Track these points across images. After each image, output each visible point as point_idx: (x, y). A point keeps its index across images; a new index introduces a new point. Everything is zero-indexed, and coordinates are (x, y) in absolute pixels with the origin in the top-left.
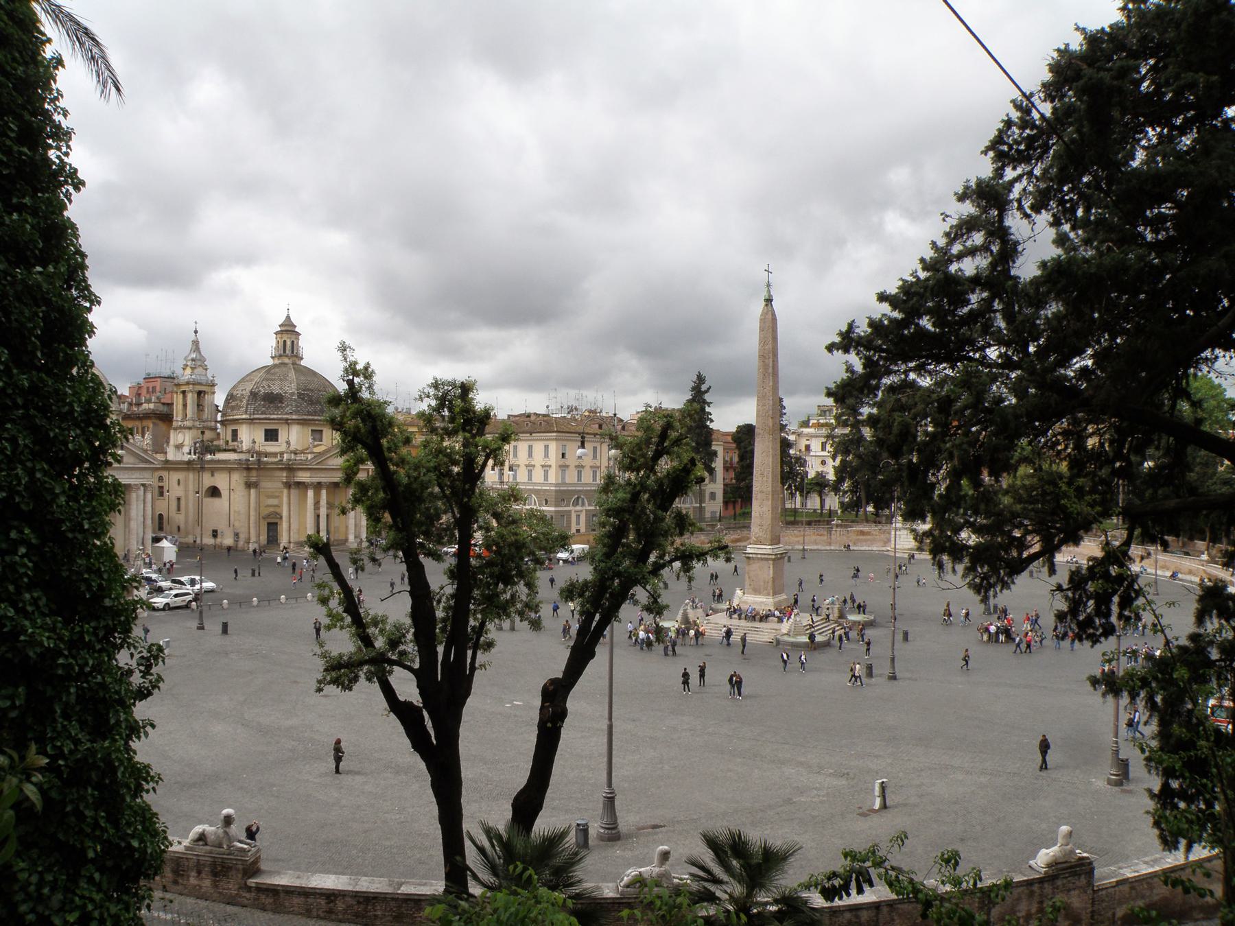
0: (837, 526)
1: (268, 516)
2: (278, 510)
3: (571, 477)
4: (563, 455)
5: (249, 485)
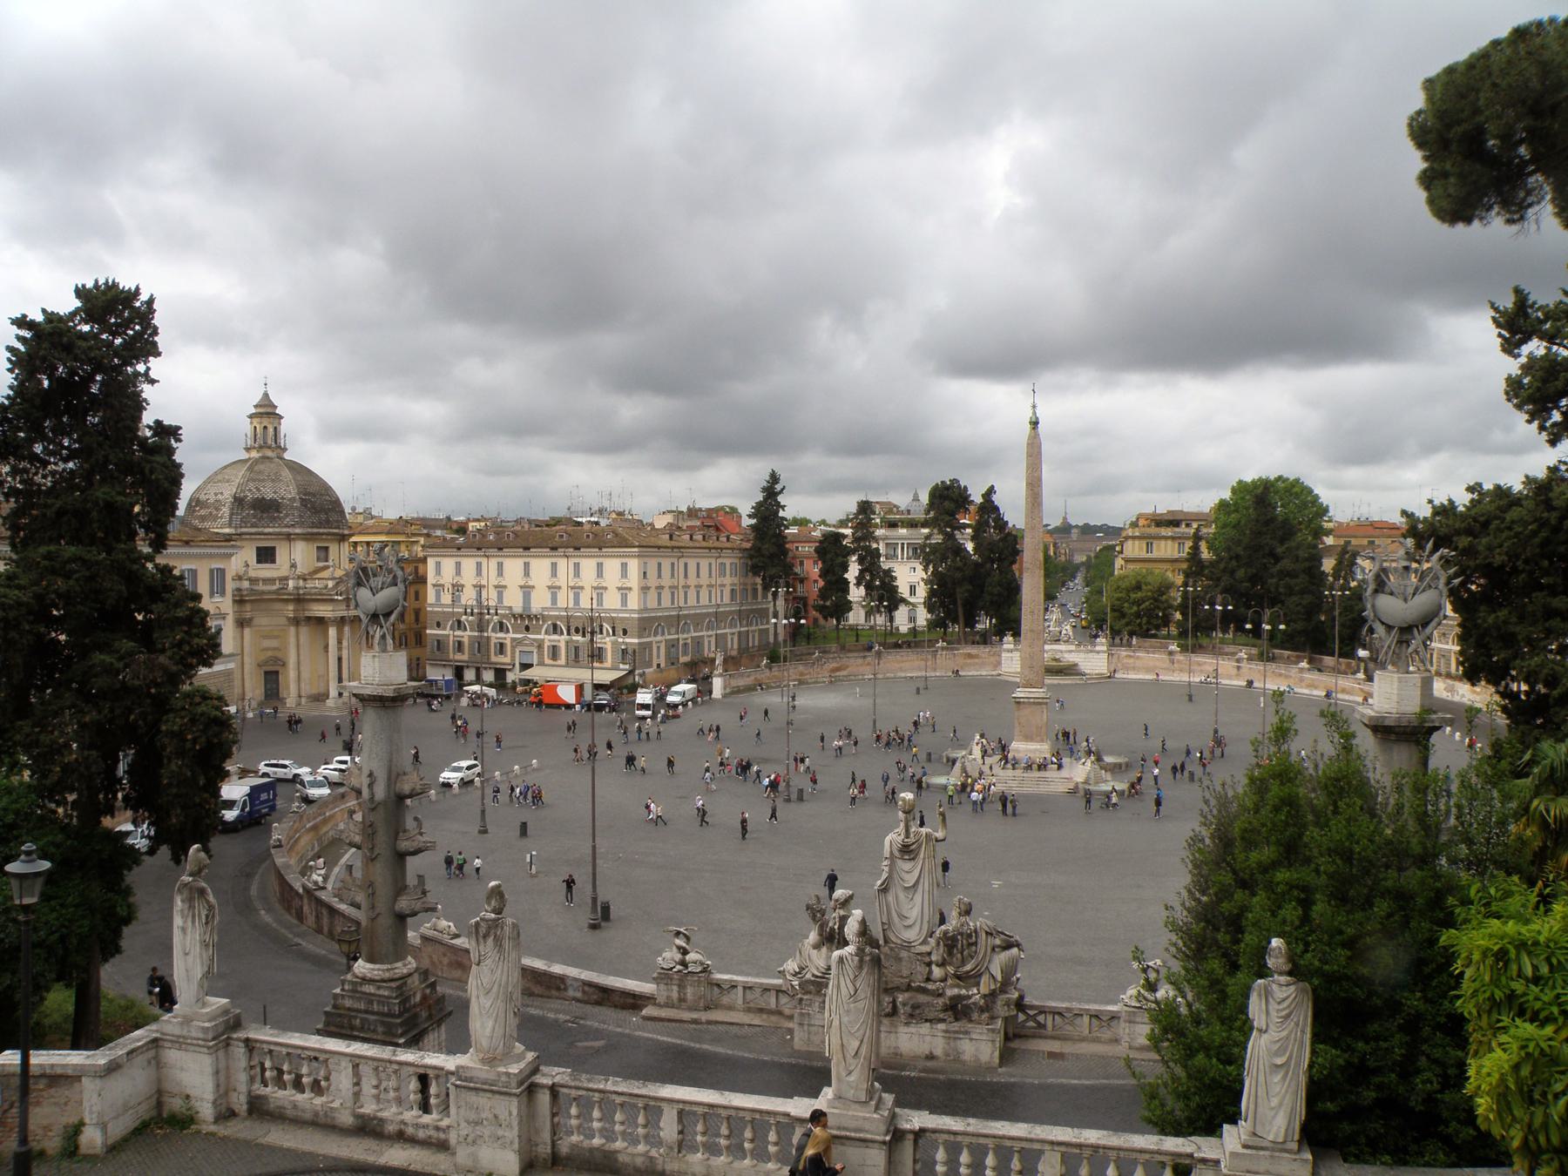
0: (943, 648)
1: (266, 663)
2: (279, 655)
3: (652, 603)
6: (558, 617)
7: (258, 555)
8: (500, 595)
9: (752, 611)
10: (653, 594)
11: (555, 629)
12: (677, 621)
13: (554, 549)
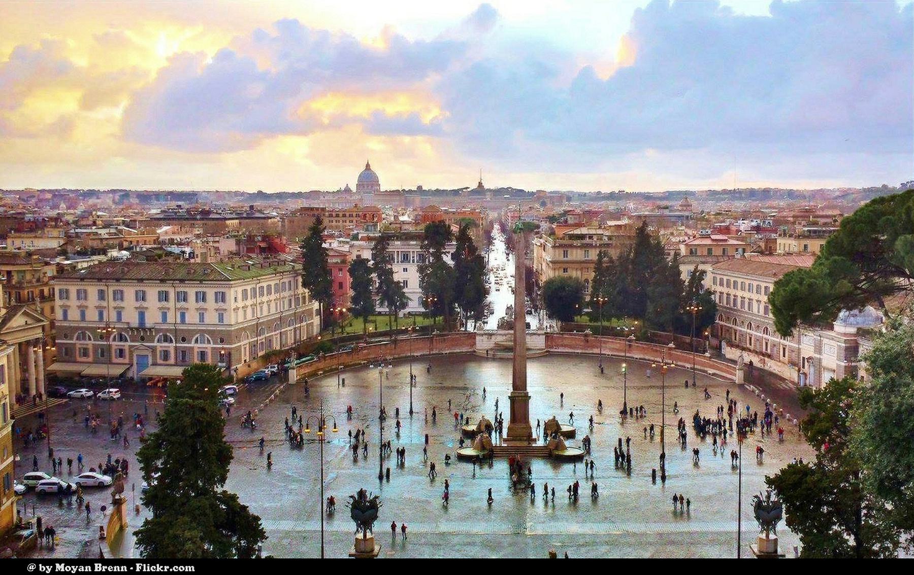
6: (167, 330)
8: (119, 315)
9: (303, 312)
10: (241, 312)
11: (166, 339)
12: (257, 329)
13: (162, 281)
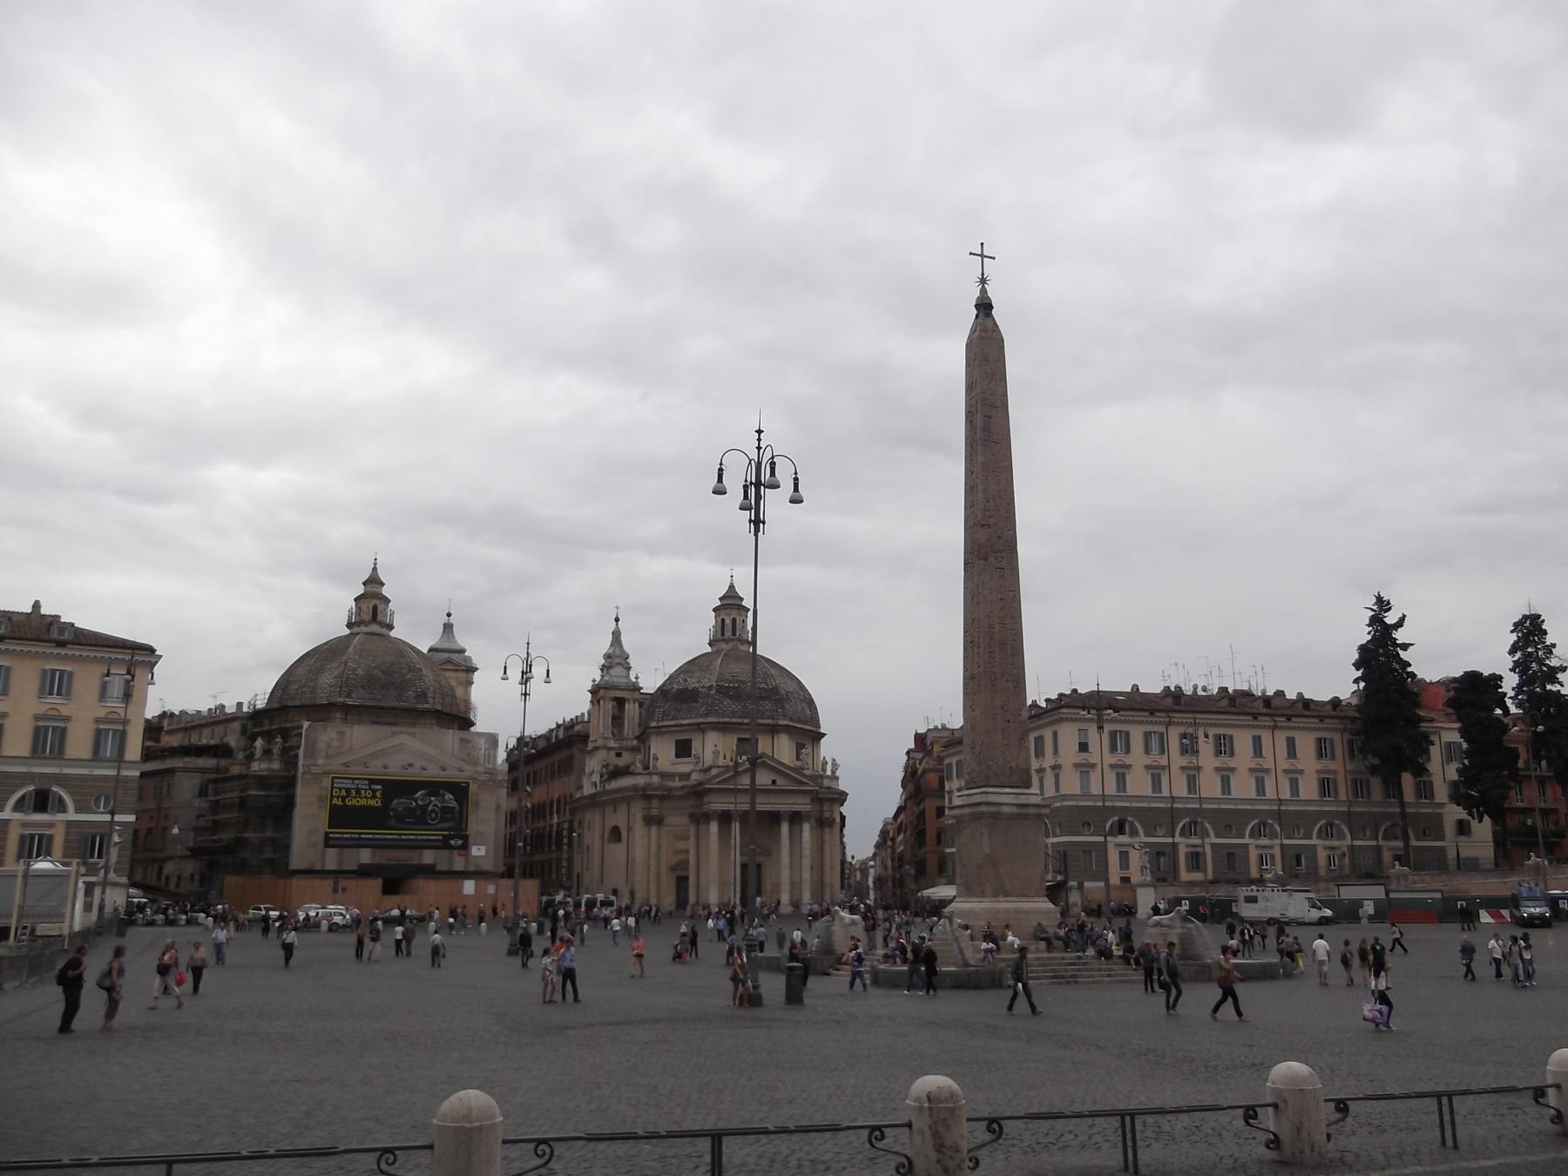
4: (1083, 747)
5: (649, 821)
7: (677, 749)
